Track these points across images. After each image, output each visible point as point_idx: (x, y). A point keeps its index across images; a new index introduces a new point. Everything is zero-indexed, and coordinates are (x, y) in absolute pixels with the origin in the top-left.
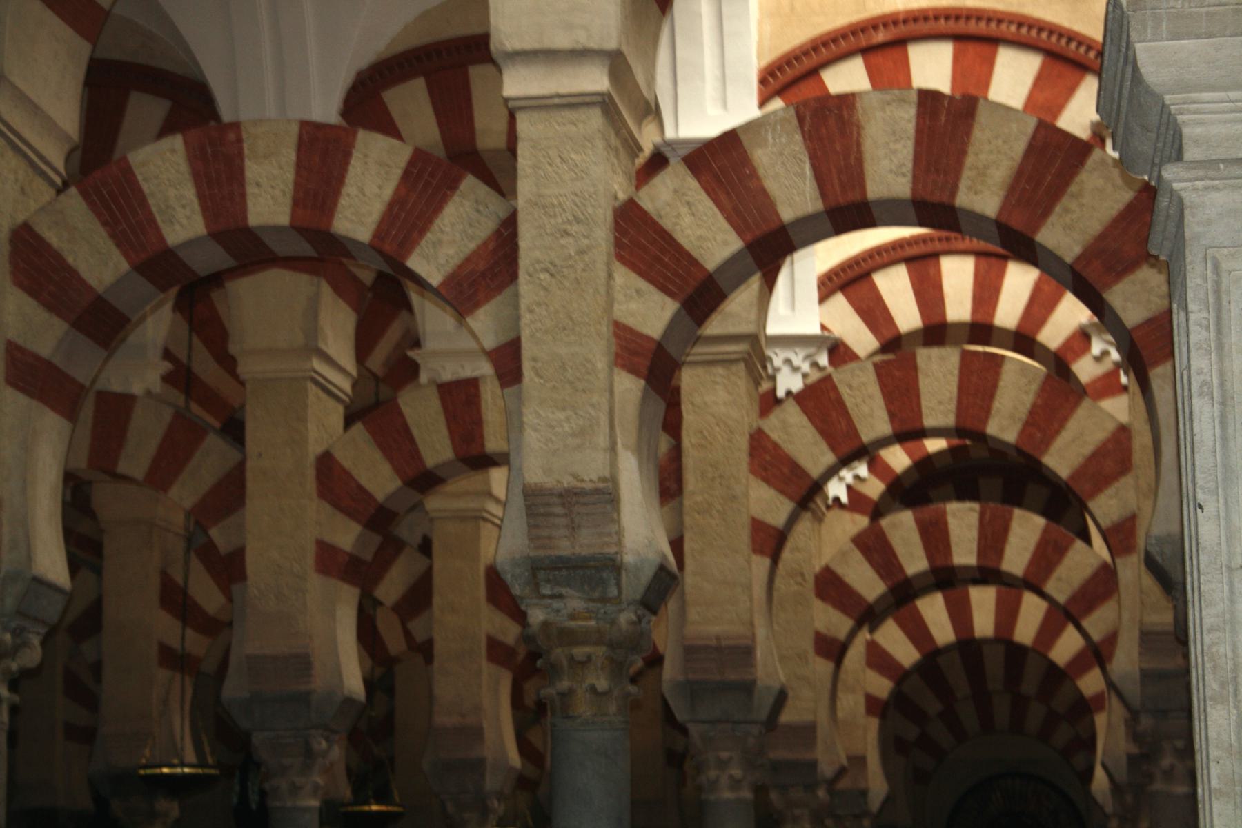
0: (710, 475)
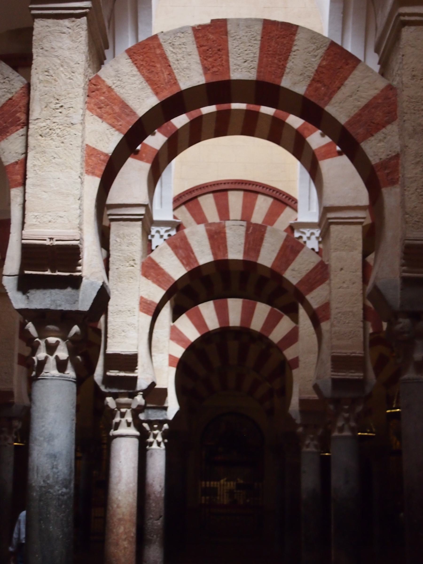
0: (53, 106)
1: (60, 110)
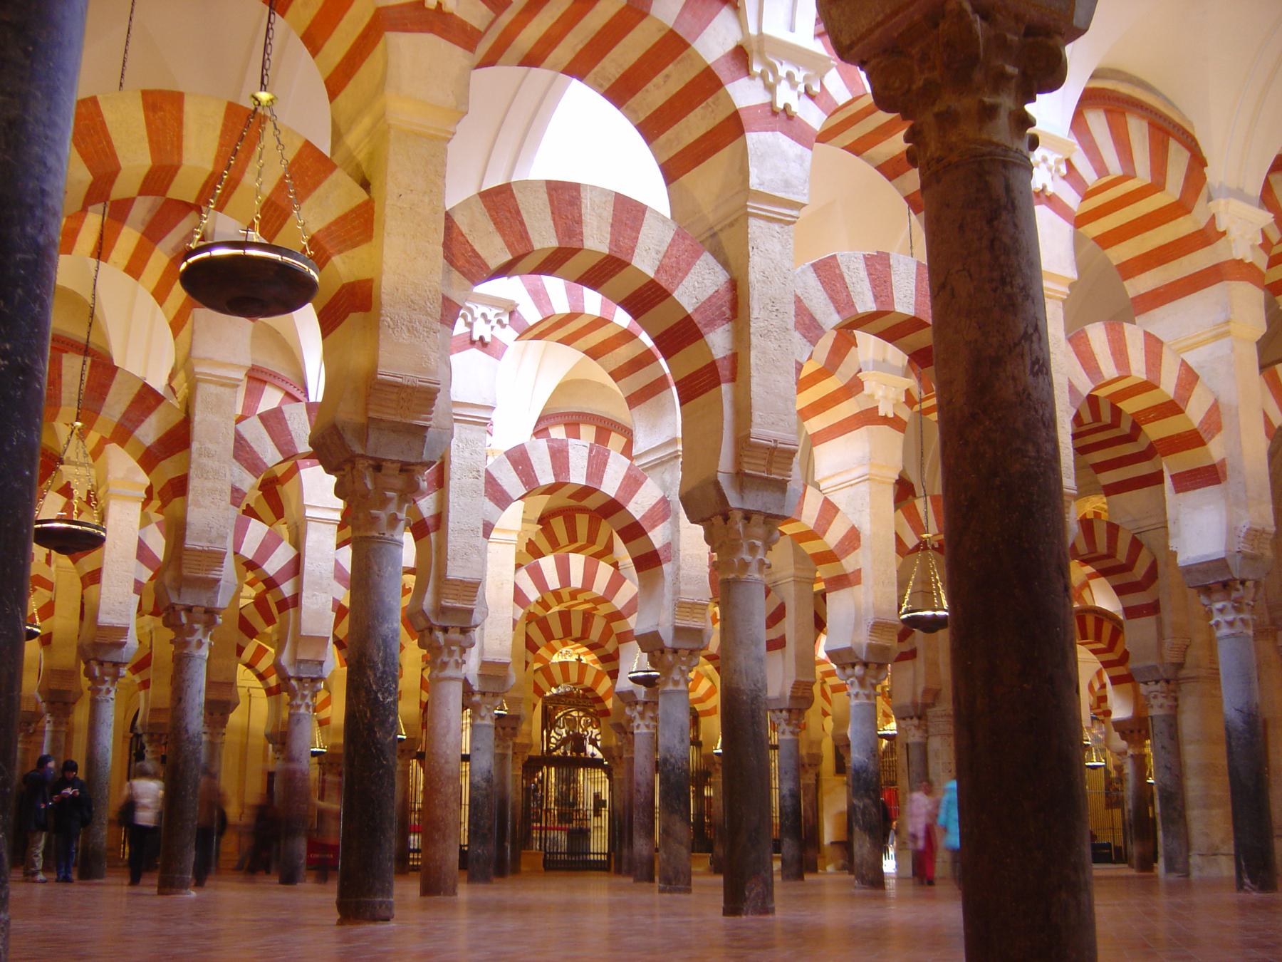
0: (770, 308)
1: (775, 313)
